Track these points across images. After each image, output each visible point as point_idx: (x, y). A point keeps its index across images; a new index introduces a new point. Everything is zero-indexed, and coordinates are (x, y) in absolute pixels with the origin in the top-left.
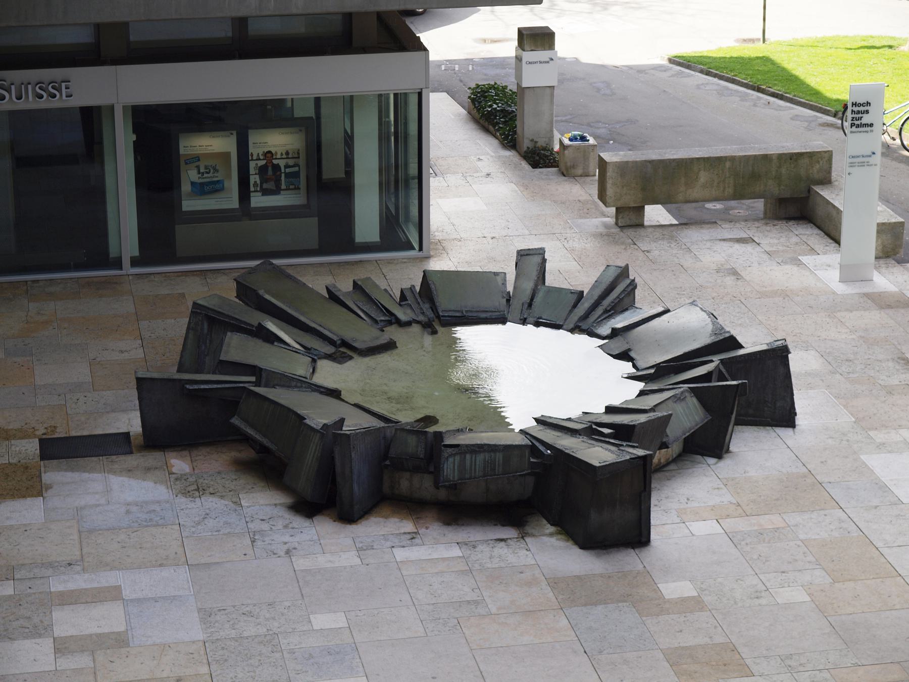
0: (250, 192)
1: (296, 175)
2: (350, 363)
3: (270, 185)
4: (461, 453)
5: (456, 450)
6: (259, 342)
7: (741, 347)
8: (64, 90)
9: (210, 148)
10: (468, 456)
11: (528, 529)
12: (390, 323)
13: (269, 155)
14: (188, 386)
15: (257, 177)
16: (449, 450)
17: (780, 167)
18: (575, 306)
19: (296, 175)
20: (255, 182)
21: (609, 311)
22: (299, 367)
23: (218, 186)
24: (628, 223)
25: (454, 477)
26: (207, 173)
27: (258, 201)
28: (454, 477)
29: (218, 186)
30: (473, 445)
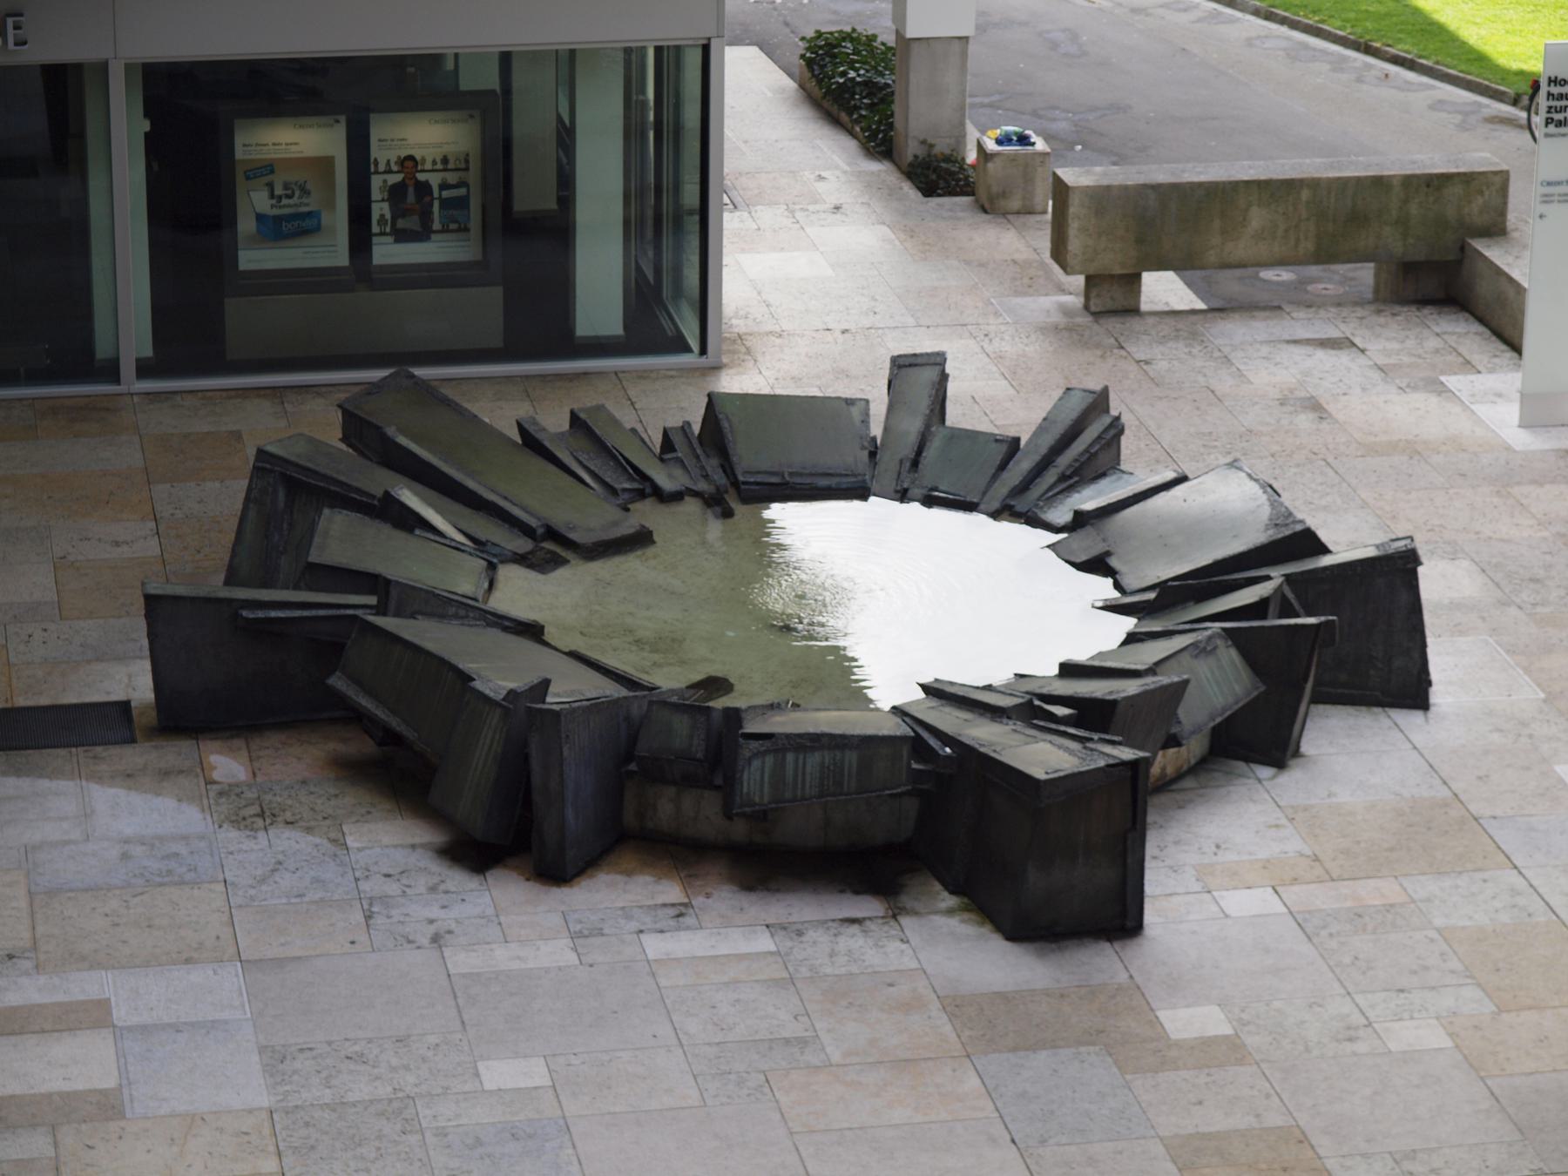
0: (370, 235)
1: (462, 203)
2: (562, 573)
4: (776, 751)
5: (768, 744)
6: (386, 529)
7: (1324, 550)
9: (294, 148)
10: (790, 757)
11: (905, 900)
12: (641, 495)
13: (409, 164)
14: (245, 613)
15: (386, 206)
16: (754, 745)
17: (1406, 201)
18: (1003, 467)
19: (462, 203)
20: (382, 216)
21: (1070, 477)
22: (464, 579)
23: (308, 223)
24: (1110, 305)
25: (762, 797)
27: (386, 252)
28: (762, 797)
29: (308, 223)
30: (800, 736)
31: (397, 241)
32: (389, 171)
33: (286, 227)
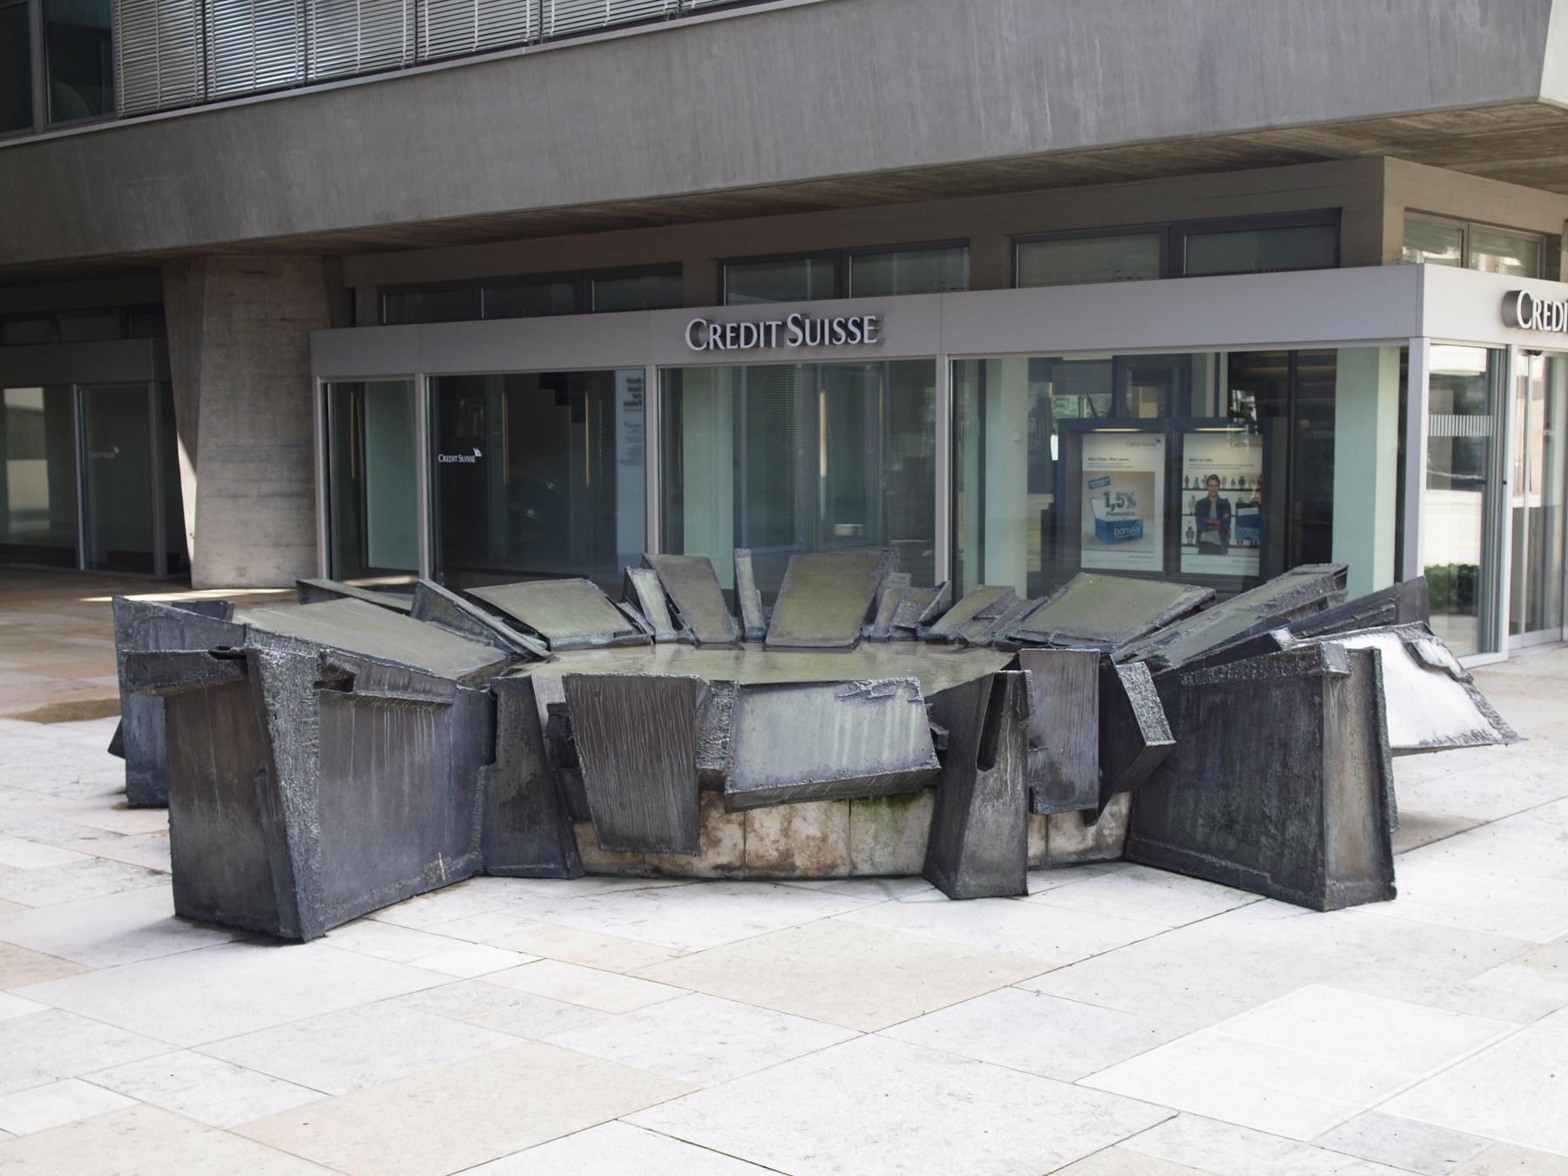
0: (1179, 545)
3: (1212, 537)
8: (866, 328)
13: (1213, 482)
15: (1193, 519)
23: (1133, 531)
26: (1120, 506)
27: (1192, 561)
29: (1133, 531)
31: (1201, 552)
32: (1197, 489)
33: (1117, 533)
